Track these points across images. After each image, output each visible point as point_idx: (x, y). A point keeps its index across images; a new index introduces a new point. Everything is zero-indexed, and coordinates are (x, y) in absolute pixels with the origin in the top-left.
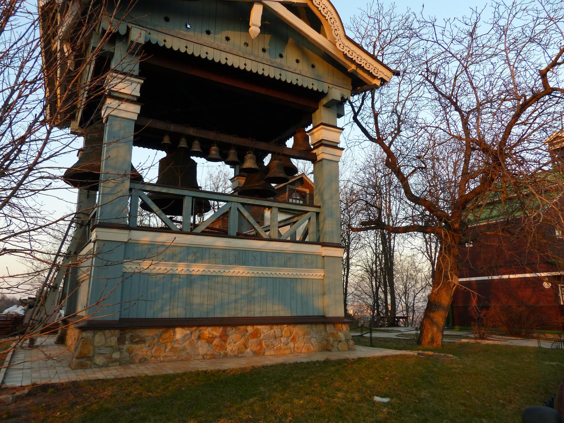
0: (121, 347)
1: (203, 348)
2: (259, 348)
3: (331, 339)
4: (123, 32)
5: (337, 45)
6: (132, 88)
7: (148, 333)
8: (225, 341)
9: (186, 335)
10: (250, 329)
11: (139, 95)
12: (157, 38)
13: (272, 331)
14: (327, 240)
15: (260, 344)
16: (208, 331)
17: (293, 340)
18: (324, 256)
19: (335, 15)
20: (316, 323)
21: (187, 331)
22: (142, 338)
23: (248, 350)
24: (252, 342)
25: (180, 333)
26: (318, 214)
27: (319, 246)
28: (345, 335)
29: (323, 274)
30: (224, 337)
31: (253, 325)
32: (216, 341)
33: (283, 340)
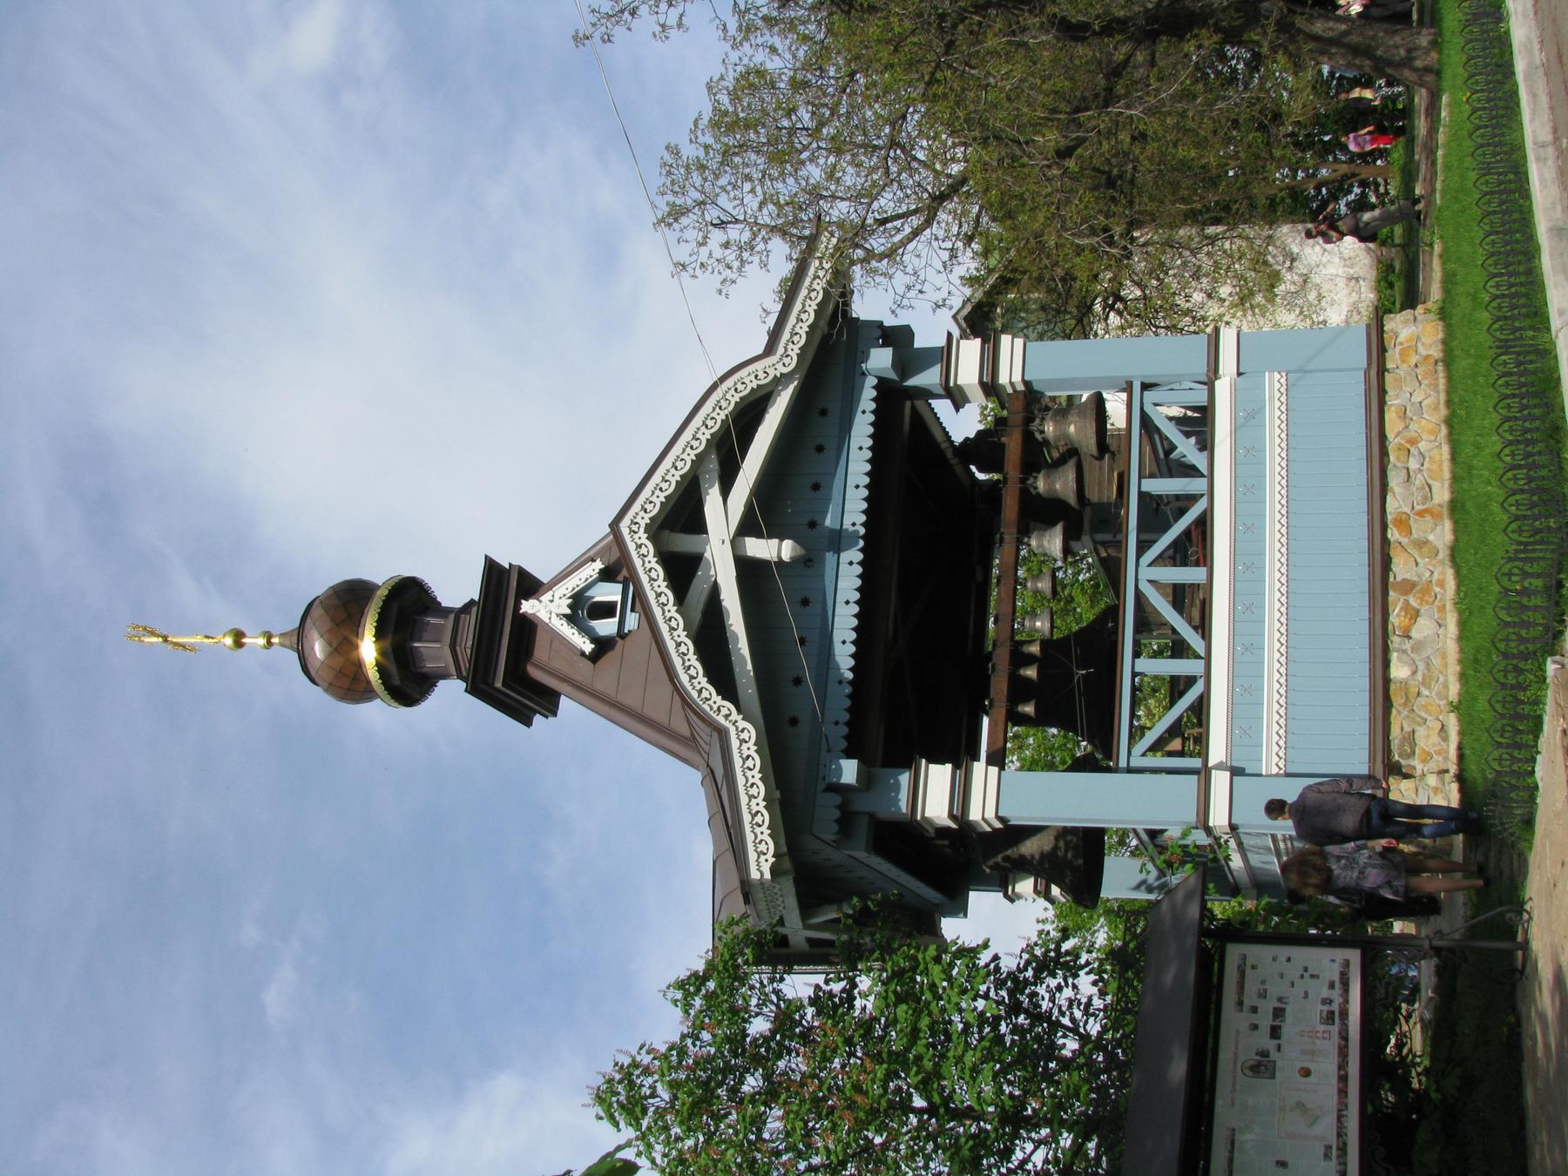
0: (1418, 772)
1: (1423, 628)
2: (1428, 518)
3: (1414, 360)
4: (838, 799)
5: (786, 370)
6: (938, 778)
7: (1395, 731)
8: (1413, 585)
9: (1399, 659)
10: (1393, 534)
11: (949, 766)
12: (838, 735)
13: (1397, 489)
14: (1201, 369)
15: (1421, 514)
16: (1396, 618)
17: (1413, 442)
18: (1239, 374)
19: (729, 383)
20: (1382, 392)
21: (1394, 656)
22: (1404, 738)
23: (1431, 537)
24: (1419, 528)
25: (1399, 671)
26: (1146, 387)
27: (1217, 383)
28: (1406, 322)
29: (1277, 376)
30: (1408, 587)
31: (1384, 527)
32: (1413, 602)
33: (1413, 464)
